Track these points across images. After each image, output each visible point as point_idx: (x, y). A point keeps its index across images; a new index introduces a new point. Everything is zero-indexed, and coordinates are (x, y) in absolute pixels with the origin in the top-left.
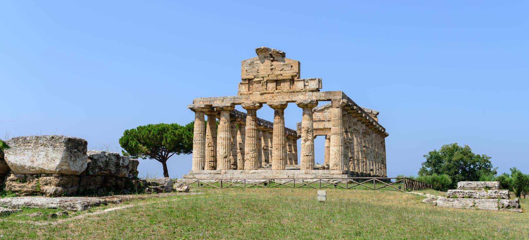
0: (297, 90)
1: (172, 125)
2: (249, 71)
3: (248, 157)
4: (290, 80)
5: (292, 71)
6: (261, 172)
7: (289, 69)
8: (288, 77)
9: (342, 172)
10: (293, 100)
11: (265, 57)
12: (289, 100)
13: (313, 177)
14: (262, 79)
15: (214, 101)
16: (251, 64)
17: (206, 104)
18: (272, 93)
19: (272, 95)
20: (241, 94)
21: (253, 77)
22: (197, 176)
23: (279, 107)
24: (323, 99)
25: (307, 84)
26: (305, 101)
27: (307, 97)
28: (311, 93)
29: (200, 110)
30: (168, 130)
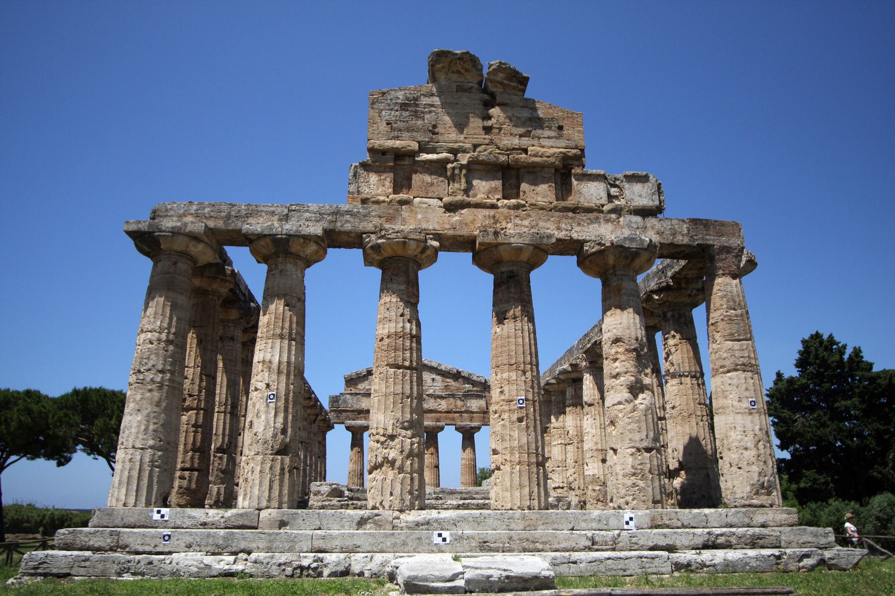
0: (586, 204)
1: (28, 393)
2: (400, 125)
3: (392, 454)
4: (557, 170)
5: (562, 143)
6: (455, 523)
7: (553, 134)
8: (552, 160)
9: (794, 518)
10: (575, 236)
11: (461, 89)
12: (561, 235)
13: (699, 541)
14: (451, 156)
15: (247, 216)
16: (410, 105)
17: (211, 224)
18: (493, 207)
19: (492, 212)
20: (364, 201)
21: (415, 146)
22: (133, 537)
23: (524, 257)
24: (686, 240)
25: (614, 191)
26: (632, 240)
27: (627, 233)
28: (638, 219)
29: (180, 244)
30: (16, 404)
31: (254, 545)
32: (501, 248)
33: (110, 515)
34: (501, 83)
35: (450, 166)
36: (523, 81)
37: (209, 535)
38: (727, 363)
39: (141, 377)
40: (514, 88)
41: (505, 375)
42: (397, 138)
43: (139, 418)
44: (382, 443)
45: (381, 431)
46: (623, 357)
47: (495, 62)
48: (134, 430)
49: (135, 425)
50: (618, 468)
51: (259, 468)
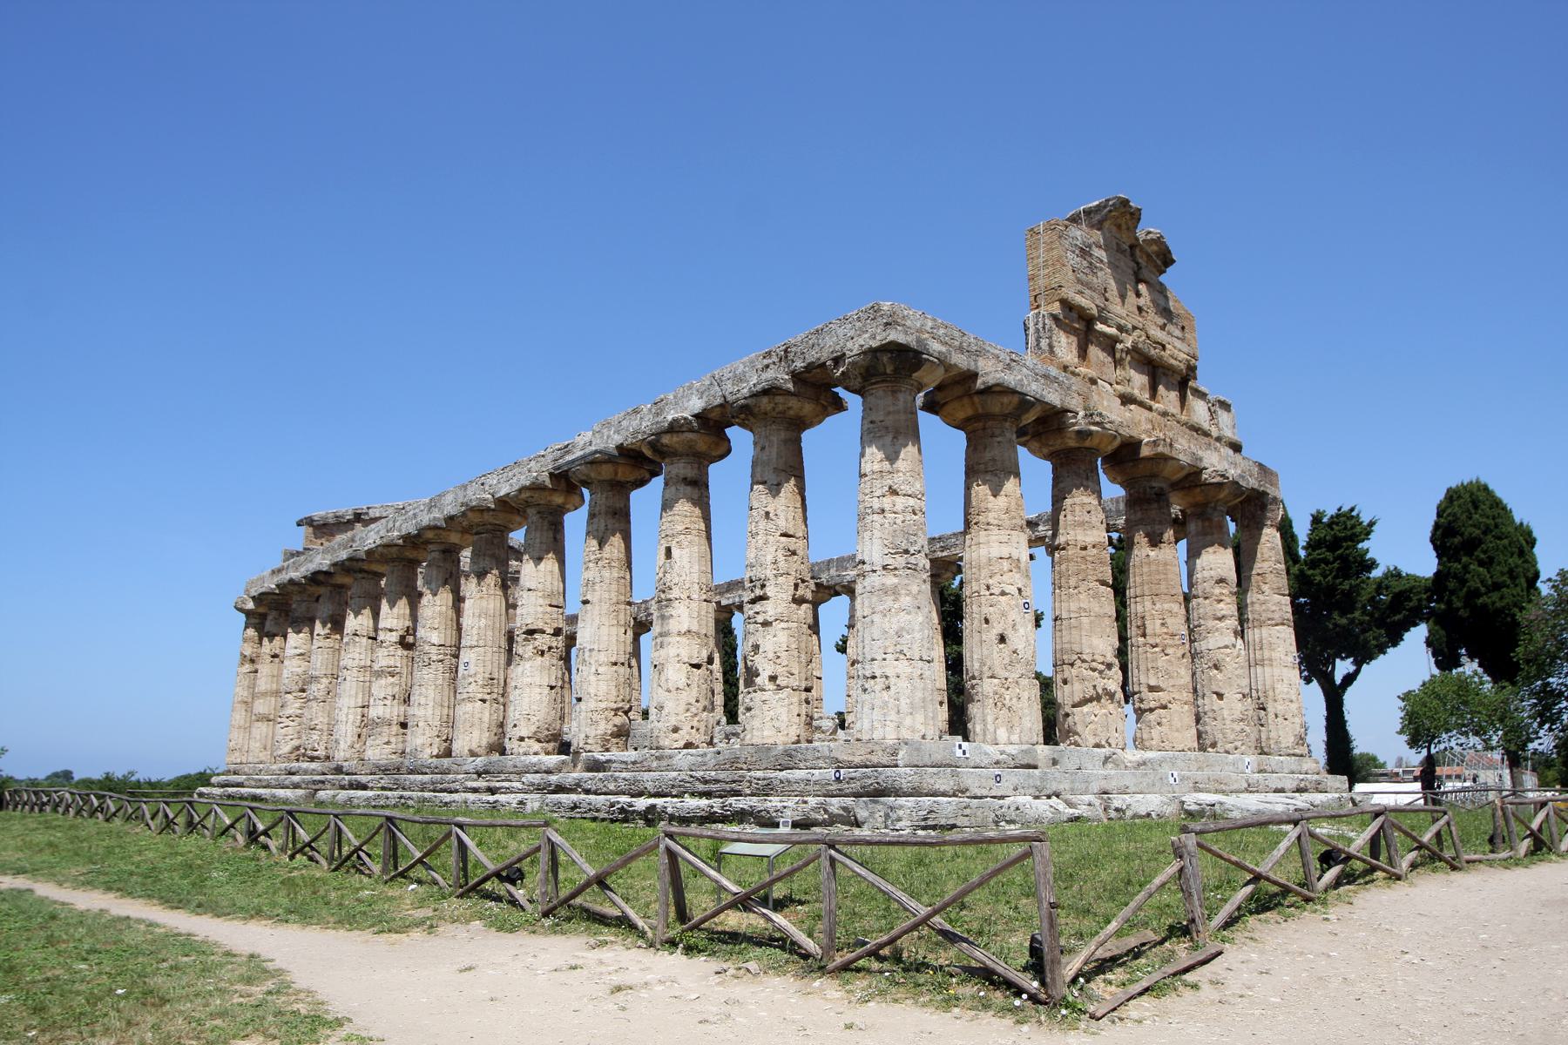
8: (1182, 366)
13: (1294, 785)
18: (1150, 409)
20: (1065, 368)
21: (1095, 312)
28: (1231, 452)
31: (1061, 787)
32: (1171, 463)
33: (918, 750)
34: (1149, 256)
35: (1119, 346)
36: (1166, 259)
37: (1029, 776)
38: (1276, 616)
39: (912, 560)
40: (1156, 266)
41: (1166, 606)
42: (1080, 293)
43: (921, 619)
44: (1101, 672)
45: (1101, 659)
46: (1228, 600)
47: (1156, 231)
48: (918, 635)
49: (917, 628)
50: (1226, 713)
51: (1025, 695)
